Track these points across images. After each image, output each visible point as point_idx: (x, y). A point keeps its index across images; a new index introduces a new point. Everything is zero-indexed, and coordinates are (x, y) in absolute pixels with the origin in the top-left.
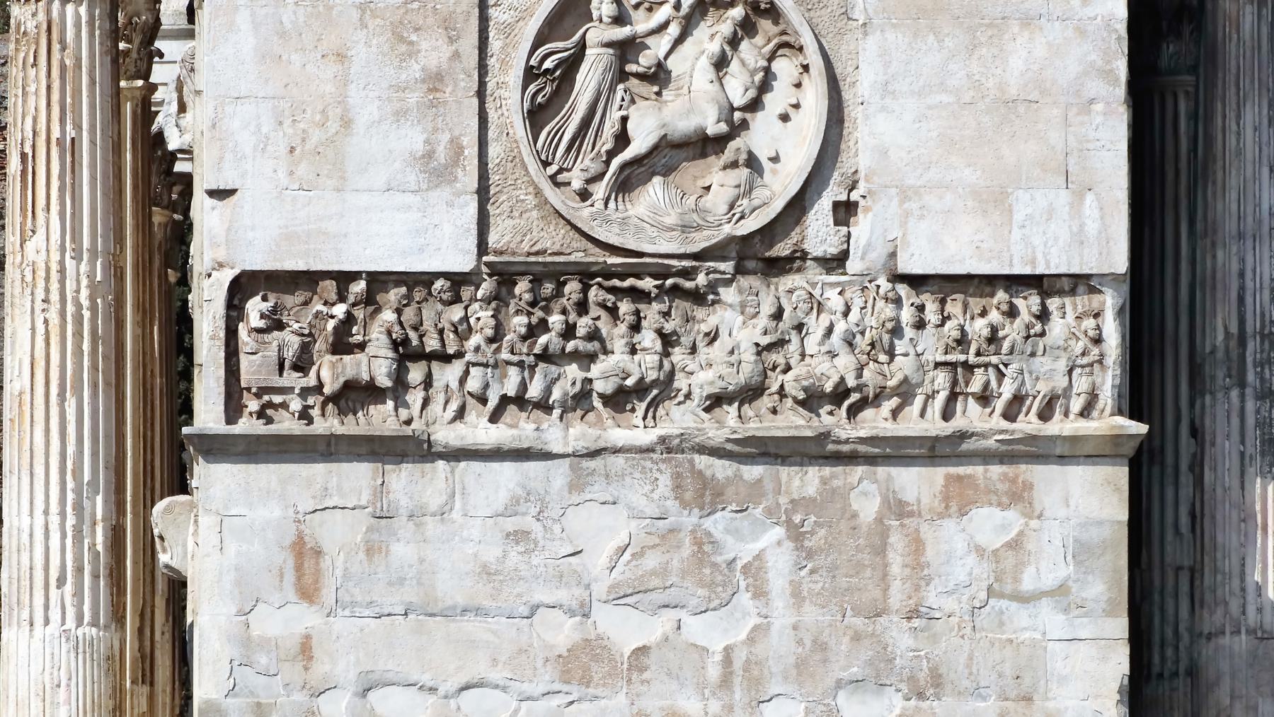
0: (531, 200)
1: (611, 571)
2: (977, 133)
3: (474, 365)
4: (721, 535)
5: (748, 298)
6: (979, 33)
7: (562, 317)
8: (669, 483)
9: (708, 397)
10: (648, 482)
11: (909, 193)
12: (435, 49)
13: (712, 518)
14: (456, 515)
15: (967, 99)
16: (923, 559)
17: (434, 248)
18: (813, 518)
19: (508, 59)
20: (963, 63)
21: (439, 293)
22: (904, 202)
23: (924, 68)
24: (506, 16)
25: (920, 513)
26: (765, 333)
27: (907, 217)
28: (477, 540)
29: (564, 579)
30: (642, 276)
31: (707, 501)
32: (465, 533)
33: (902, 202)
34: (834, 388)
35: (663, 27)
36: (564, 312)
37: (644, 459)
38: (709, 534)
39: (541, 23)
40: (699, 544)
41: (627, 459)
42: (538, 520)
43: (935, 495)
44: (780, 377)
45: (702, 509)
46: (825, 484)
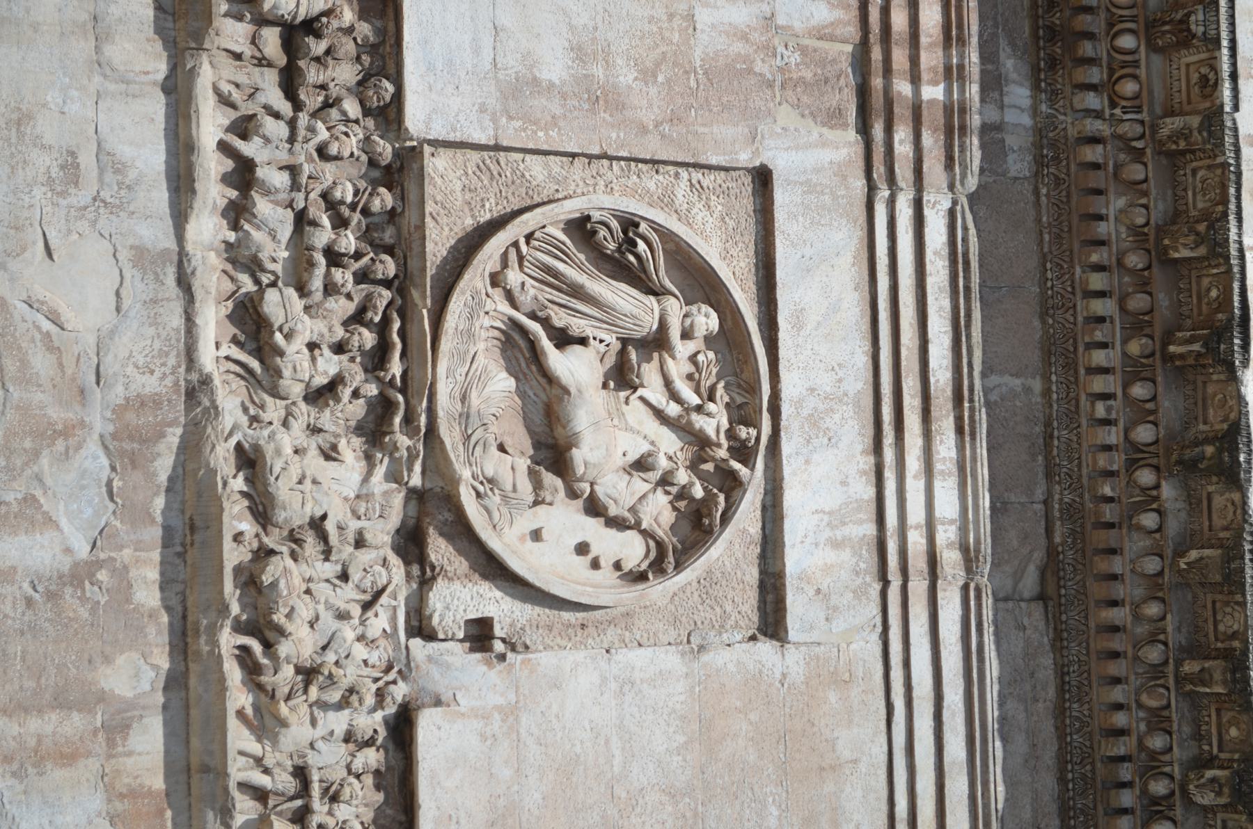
0: (485, 217)
1: (24, 301)
2: (580, 806)
3: (292, 124)
4: (76, 465)
5: (377, 505)
6: (687, 800)
7: (352, 252)
8: (147, 390)
9: (257, 448)
10: (148, 359)
11: (511, 719)
12: (650, 106)
13: (101, 453)
14: (97, 79)
15: (620, 792)
16: (49, 766)
17: (432, 82)
18: (103, 600)
19: (637, 197)
20: (655, 781)
21: (375, 85)
22: (500, 713)
23: (648, 732)
24: (680, 196)
25: (114, 756)
26: (340, 528)
27: (483, 718)
28: (66, 110)
29: (12, 232)
30: (405, 359)
31: (124, 444)
32: (75, 93)
33: (499, 708)
34: (277, 625)
35: (674, 396)
36: (358, 256)
37: (178, 356)
38: (79, 447)
39: (684, 237)
40: (66, 433)
41: (177, 330)
42: (95, 199)
43: (137, 777)
44: (285, 549)
45: (114, 436)
46: (150, 616)
